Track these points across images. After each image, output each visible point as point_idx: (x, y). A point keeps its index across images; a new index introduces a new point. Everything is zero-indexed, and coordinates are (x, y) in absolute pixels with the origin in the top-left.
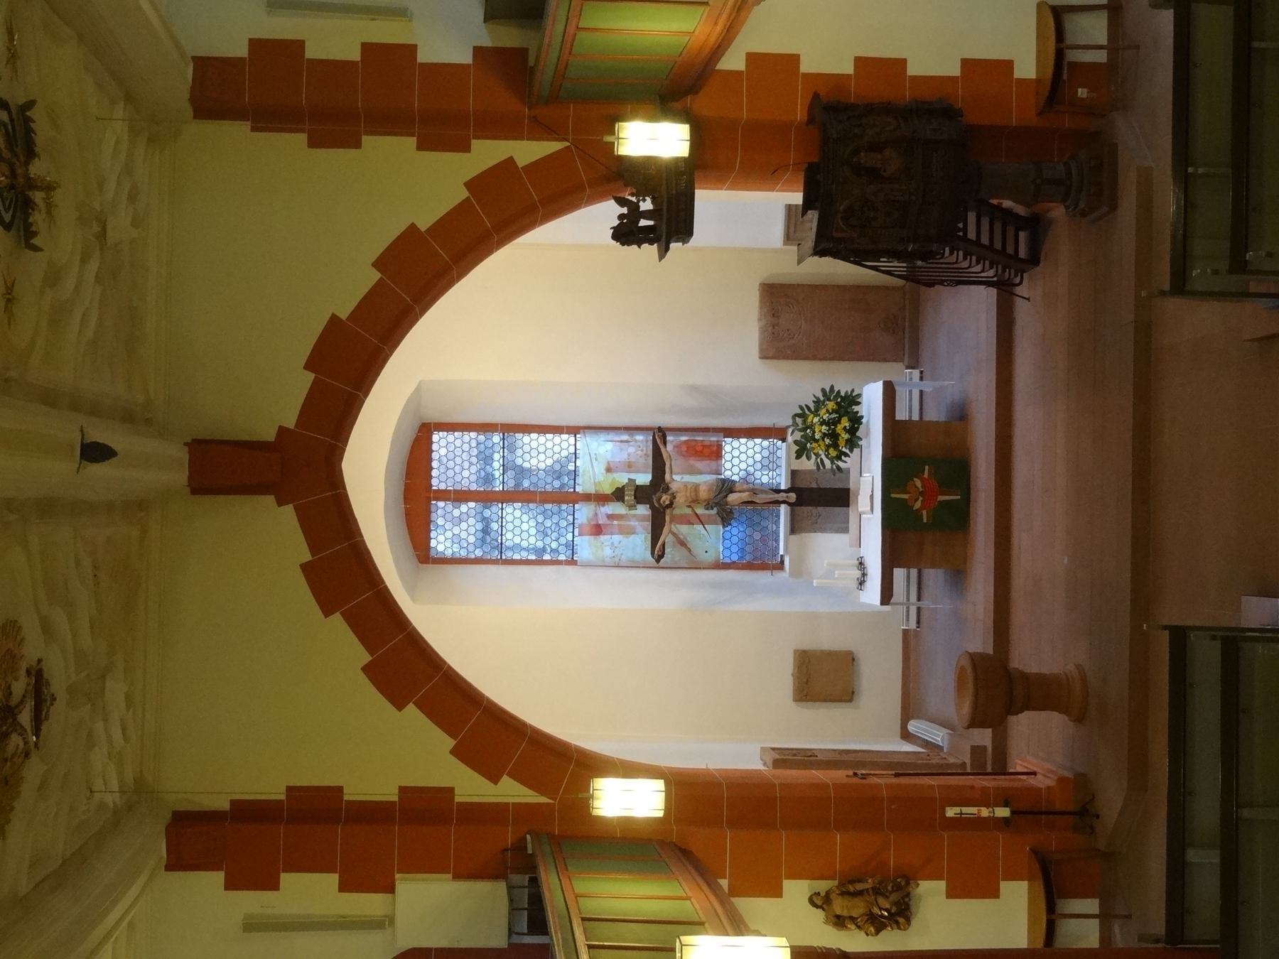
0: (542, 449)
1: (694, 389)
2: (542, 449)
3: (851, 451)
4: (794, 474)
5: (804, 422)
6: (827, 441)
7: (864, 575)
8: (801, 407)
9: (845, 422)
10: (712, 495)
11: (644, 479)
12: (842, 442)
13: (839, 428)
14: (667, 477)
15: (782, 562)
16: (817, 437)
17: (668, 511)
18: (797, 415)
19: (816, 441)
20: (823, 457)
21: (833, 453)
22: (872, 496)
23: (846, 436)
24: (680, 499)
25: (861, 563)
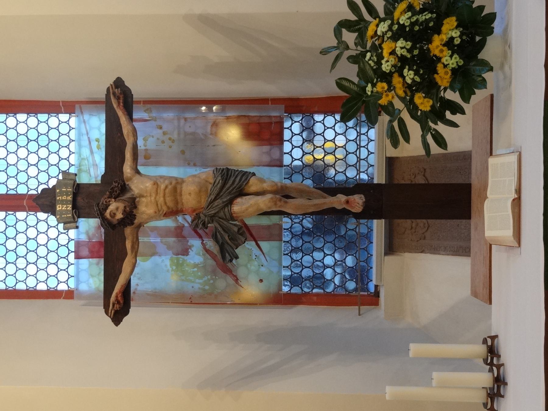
0: (33, 135)
1: (207, 23)
2: (33, 135)
3: (466, 99)
4: (391, 162)
5: (361, 40)
6: (409, 75)
7: (500, 381)
8: (353, 6)
9: (450, 29)
10: (204, 203)
11: (93, 168)
12: (443, 77)
13: (436, 45)
14: (127, 169)
15: (377, 294)
16: (386, 67)
17: (128, 231)
18: (344, 24)
19: (386, 77)
20: (406, 116)
21: (424, 103)
22: (517, 203)
23: (452, 61)
24: (145, 209)
25: (492, 351)
